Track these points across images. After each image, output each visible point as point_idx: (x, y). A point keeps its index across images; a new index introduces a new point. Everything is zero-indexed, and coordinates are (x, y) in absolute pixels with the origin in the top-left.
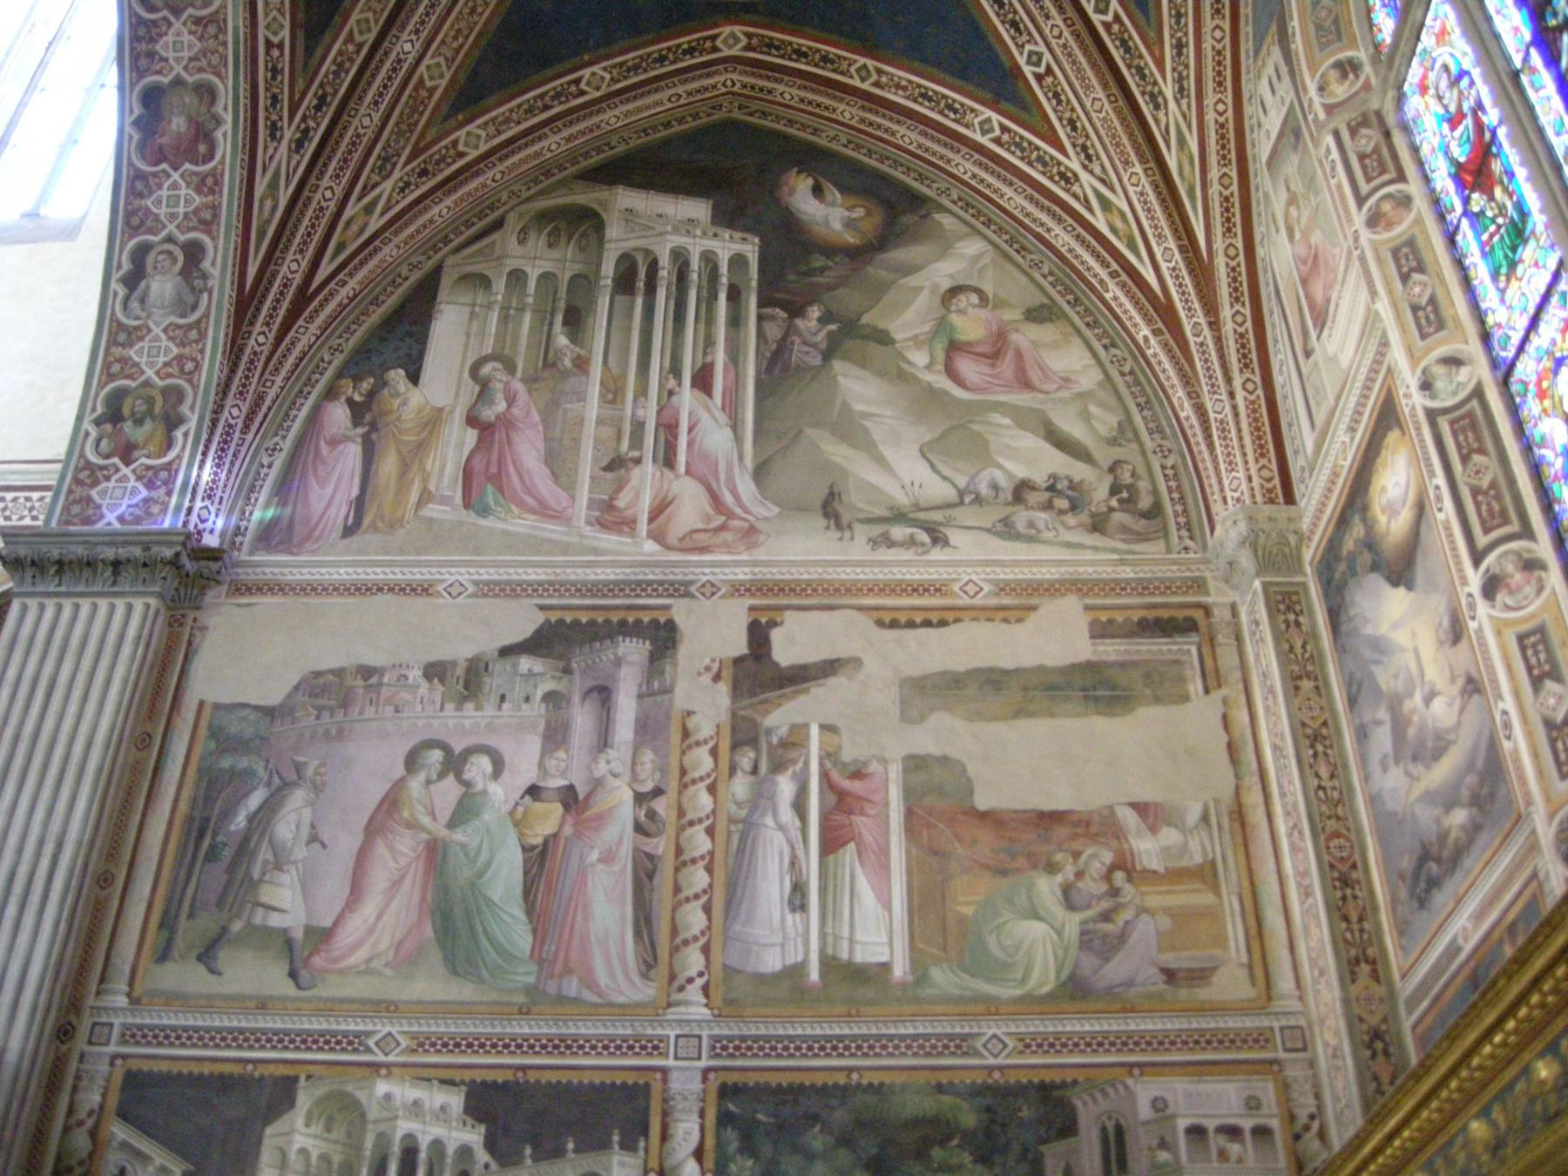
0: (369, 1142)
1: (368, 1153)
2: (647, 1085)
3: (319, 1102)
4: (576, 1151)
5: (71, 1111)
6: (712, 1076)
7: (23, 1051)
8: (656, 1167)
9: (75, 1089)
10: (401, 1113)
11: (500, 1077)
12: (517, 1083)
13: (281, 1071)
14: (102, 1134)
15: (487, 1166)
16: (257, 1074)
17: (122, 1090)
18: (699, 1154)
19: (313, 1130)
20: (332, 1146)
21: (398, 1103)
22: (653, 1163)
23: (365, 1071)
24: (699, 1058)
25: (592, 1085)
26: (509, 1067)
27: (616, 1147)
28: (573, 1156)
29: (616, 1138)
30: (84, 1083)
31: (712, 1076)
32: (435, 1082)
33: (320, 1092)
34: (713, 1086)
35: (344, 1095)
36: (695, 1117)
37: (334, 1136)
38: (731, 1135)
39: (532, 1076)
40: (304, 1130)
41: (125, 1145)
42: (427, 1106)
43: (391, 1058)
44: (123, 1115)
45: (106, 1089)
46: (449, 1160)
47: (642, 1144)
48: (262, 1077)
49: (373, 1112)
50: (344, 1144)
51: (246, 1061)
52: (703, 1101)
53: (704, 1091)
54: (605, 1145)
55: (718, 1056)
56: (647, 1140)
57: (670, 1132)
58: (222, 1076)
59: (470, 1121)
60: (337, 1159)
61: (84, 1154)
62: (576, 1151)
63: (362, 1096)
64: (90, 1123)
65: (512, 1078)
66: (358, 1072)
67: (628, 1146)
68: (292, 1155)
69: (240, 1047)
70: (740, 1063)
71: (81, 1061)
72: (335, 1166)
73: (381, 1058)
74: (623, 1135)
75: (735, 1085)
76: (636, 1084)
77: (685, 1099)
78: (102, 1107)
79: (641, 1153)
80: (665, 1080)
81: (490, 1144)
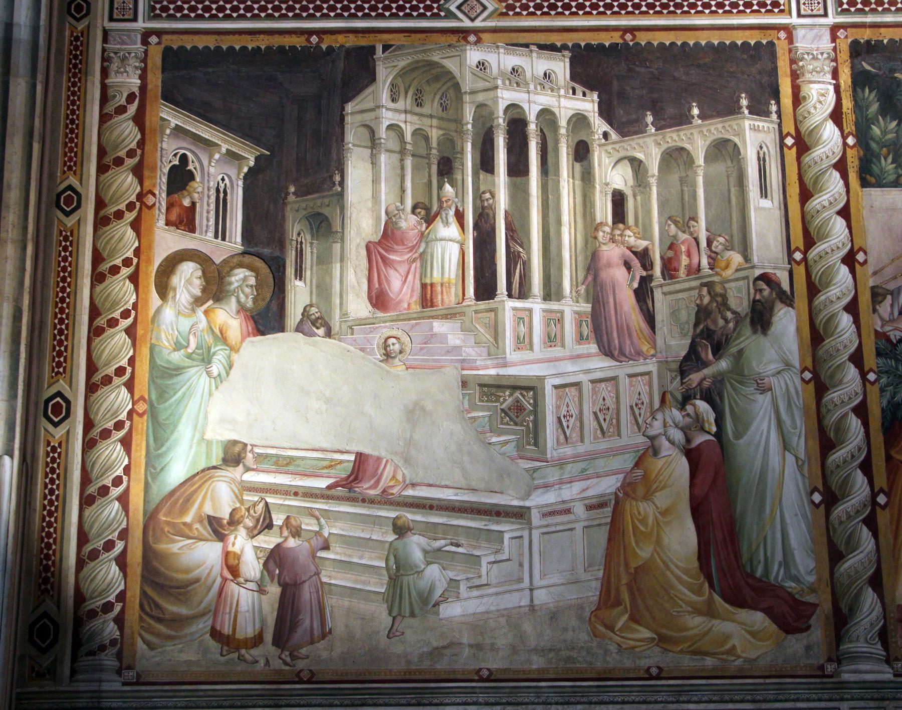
0: (469, 115)
1: (470, 126)
2: (771, 44)
3: (404, 73)
4: (702, 117)
5: (105, 99)
6: (841, 33)
7: (35, 29)
8: (793, 132)
9: (105, 73)
10: (499, 82)
11: (607, 40)
12: (626, 44)
13: (351, 41)
14: (150, 120)
15: (606, 135)
16: (324, 46)
17: (163, 72)
18: (836, 116)
19: (400, 105)
20: (428, 121)
21: (495, 71)
22: (789, 127)
23: (452, 39)
24: (826, 15)
25: (709, 45)
26: (615, 29)
27: (746, 112)
28: (700, 122)
29: (744, 102)
30: (114, 67)
31: (841, 33)
32: (534, 48)
33: (402, 63)
34: (844, 46)
35: (432, 65)
36: (828, 77)
37: (426, 110)
38: (869, 96)
39: (643, 39)
40: (392, 105)
41: (178, 128)
42: (528, 75)
43: (478, 23)
44: (169, 96)
45: (144, 71)
46: (563, 131)
47: (774, 108)
48: (330, 49)
49: (467, 84)
50: (441, 119)
51: (310, 32)
52: (835, 60)
53: (835, 49)
54: (733, 110)
55: (845, 11)
56: (778, 103)
57: (802, 94)
58: (281, 49)
59: (579, 89)
60: (435, 135)
61: (133, 145)
62: (702, 117)
63: (451, 65)
64: (132, 109)
65: (621, 41)
66: (443, 39)
67: (760, 111)
68: (382, 133)
69: (297, 17)
70: (870, 19)
71: (105, 40)
72: (434, 144)
73: (467, 23)
74: (751, 98)
75: (868, 42)
76: (758, 44)
77: (815, 58)
78: (143, 88)
79: (774, 117)
80: (790, 39)
81: (606, 112)
